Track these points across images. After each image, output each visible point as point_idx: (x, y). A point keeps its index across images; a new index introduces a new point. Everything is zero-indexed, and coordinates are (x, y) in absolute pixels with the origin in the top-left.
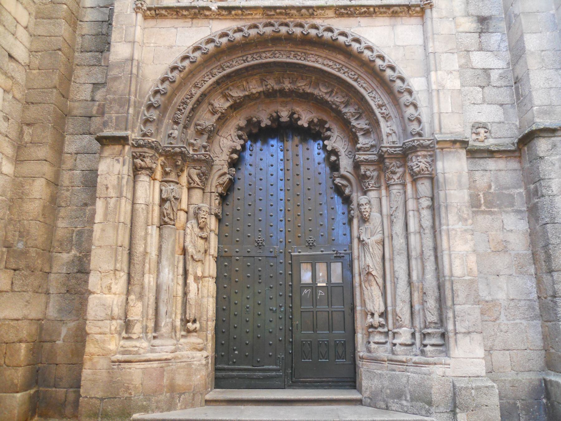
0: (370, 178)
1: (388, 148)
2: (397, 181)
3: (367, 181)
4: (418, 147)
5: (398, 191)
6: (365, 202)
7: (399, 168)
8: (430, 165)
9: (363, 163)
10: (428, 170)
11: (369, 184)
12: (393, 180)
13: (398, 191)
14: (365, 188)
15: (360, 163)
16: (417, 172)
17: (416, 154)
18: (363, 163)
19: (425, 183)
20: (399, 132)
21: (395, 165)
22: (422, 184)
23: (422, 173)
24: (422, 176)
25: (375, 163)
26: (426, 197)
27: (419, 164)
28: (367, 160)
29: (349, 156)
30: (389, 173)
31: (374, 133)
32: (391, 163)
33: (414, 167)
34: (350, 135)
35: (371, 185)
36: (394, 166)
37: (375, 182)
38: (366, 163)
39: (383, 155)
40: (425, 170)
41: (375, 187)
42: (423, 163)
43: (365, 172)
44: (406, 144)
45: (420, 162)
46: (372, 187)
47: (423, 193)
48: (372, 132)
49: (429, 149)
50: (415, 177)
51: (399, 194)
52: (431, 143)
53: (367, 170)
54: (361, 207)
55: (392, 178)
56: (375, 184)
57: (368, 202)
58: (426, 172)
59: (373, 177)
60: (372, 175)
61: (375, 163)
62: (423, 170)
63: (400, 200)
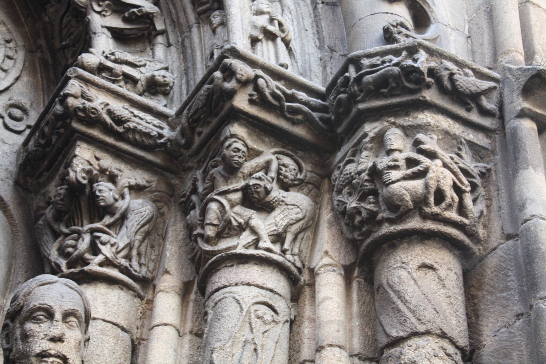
0: (108, 220)
1: (260, 72)
2: (266, 243)
3: (87, 227)
4: (428, 86)
5: (266, 296)
6: (68, 306)
7: (285, 187)
8: (474, 187)
9: (95, 133)
10: (462, 210)
11: (94, 250)
12: (246, 237)
13: (266, 296)
14: (63, 263)
15: (76, 125)
16: (408, 198)
17: (407, 121)
18: (95, 133)
19: (442, 272)
20: (303, 53)
21: (274, 166)
22: (424, 266)
23: (435, 209)
24: (430, 225)
25: (149, 157)
26: (443, 336)
27: (426, 161)
28: (119, 121)
29: (8, 121)
30: (237, 196)
31: (169, 45)
32: (253, 153)
33: (395, 175)
34: (39, 47)
35: (107, 251)
36: (266, 167)
37: (130, 246)
38: (110, 140)
39: (232, 94)
40: (448, 200)
41: (125, 271)
42: (445, 165)
43: (93, 180)
44: (366, 62)
45: (432, 155)
46: (107, 263)
47: (429, 314)
48: (160, 39)
49: (474, 117)
50: (386, 229)
51: (268, 315)
52: (487, 92)
53: (103, 171)
54: (30, 326)
55: (242, 228)
56: (128, 257)
57: (82, 313)
58: (453, 215)
59: (124, 217)
60: (122, 205)
61: (149, 157)
62: (440, 196)
63: (270, 343)
